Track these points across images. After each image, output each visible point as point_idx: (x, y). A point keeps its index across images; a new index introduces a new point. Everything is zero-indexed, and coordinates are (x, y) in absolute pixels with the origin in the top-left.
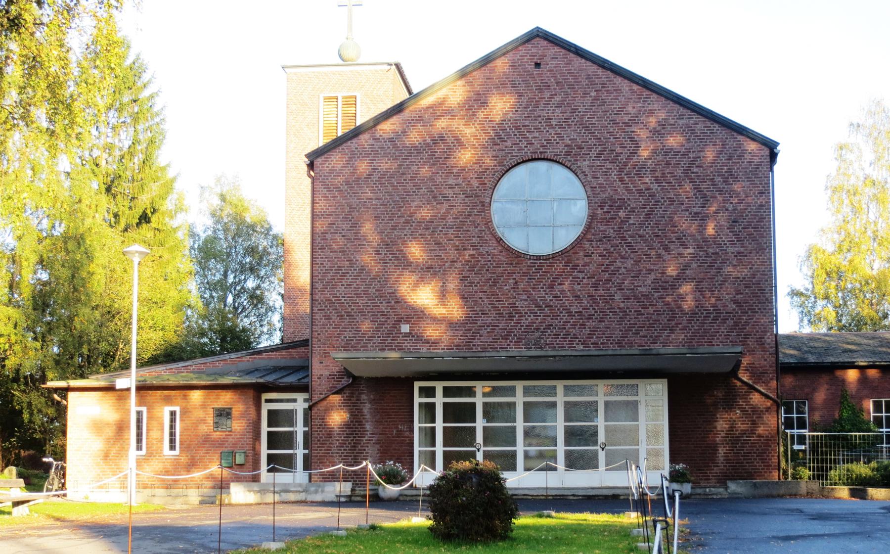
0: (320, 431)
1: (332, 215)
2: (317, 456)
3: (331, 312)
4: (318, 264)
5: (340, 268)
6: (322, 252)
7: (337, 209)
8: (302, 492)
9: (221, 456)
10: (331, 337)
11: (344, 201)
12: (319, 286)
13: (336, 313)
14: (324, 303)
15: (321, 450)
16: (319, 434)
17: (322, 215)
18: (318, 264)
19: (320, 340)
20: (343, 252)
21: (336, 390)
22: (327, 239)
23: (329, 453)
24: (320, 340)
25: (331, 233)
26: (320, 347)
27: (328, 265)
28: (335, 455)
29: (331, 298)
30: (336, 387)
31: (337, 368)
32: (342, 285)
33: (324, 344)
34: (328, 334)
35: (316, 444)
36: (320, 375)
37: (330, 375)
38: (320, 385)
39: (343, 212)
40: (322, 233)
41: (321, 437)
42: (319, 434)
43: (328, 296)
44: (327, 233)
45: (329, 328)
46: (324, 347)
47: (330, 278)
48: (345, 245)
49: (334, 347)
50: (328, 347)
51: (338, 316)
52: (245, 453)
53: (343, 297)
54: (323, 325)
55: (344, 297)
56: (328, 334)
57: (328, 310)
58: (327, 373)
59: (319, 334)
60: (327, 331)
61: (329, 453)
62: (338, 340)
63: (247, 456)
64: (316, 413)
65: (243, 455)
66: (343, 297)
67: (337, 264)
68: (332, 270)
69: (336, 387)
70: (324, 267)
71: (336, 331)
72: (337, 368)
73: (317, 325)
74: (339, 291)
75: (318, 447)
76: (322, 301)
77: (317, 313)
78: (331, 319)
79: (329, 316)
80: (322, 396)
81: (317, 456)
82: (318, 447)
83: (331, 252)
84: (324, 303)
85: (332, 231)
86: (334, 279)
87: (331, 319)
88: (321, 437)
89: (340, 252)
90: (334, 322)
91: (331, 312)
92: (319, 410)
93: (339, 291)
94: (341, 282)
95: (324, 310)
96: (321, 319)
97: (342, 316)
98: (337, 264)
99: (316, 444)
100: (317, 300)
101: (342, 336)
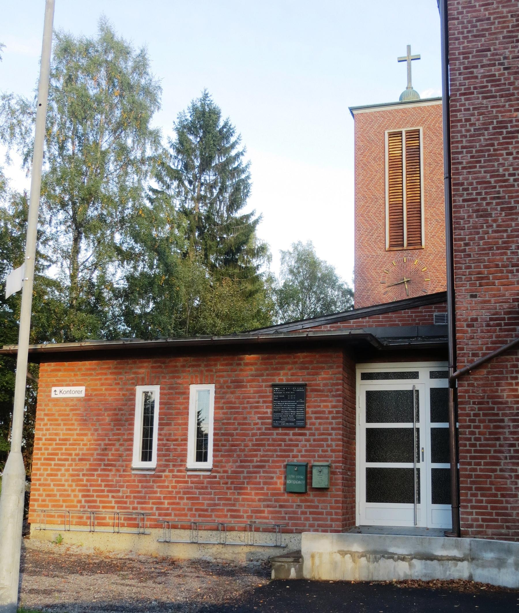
0: (476, 427)
1: (483, 36)
2: (470, 476)
3: (488, 204)
4: (460, 121)
5: (502, 125)
6: (466, 99)
7: (493, 23)
8: (461, 560)
9: (285, 472)
10: (490, 249)
11: (505, 10)
12: (465, 158)
13: (498, 204)
14: (476, 189)
15: (479, 464)
16: (473, 433)
17: (464, 38)
18: (460, 121)
19: (469, 256)
20: (507, 95)
21: (505, 347)
22: (476, 77)
23: (495, 471)
24: (469, 256)
25: (482, 66)
26: (469, 267)
27: (478, 121)
28: (507, 474)
29: (488, 178)
30: (505, 342)
31: (505, 306)
32: (511, 154)
33: (479, 261)
34: (485, 243)
35: (469, 451)
36: (473, 320)
37: (491, 319)
38: (472, 338)
39: (503, 28)
40: (466, 68)
41: (477, 439)
42: (473, 433)
43: (483, 174)
44: (476, 67)
45: (487, 233)
46: (478, 267)
47: (483, 143)
48: (510, 84)
49: (497, 266)
50: (485, 267)
51: (502, 209)
52: (329, 466)
53: (510, 175)
54: (475, 228)
55: (514, 175)
56: (485, 243)
57: (484, 199)
58: (485, 315)
59: (466, 245)
60: (482, 238)
61: (495, 471)
62: (506, 254)
63: (333, 473)
64: (467, 391)
65: (326, 471)
66: (510, 175)
67: (496, 117)
68: (487, 129)
69: (505, 342)
70: (471, 125)
71: (502, 237)
72: (505, 306)
73: (463, 229)
74: (503, 165)
75: (472, 458)
76: (471, 184)
77: (461, 207)
78: (490, 215)
79: (486, 210)
80: (477, 360)
81: (470, 476)
82: (472, 458)
83: (484, 98)
84: (476, 189)
85: (485, 61)
86: (493, 145)
87: (490, 215)
88: (477, 439)
89: (502, 96)
90: (495, 221)
91: (488, 204)
92: (472, 385)
93: (503, 165)
94: (506, 149)
95: (475, 200)
96: (470, 217)
97: (512, 208)
98: (496, 117)
99: (469, 451)
100: (462, 184)
101: (514, 246)
